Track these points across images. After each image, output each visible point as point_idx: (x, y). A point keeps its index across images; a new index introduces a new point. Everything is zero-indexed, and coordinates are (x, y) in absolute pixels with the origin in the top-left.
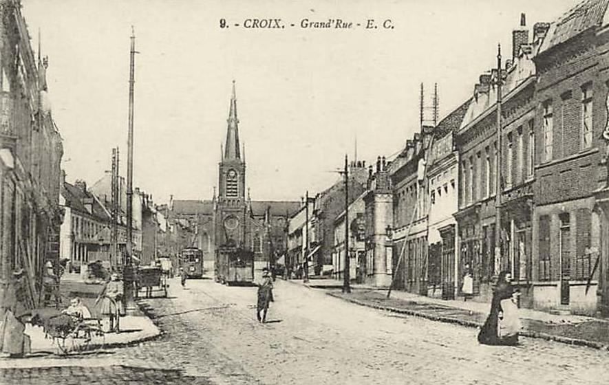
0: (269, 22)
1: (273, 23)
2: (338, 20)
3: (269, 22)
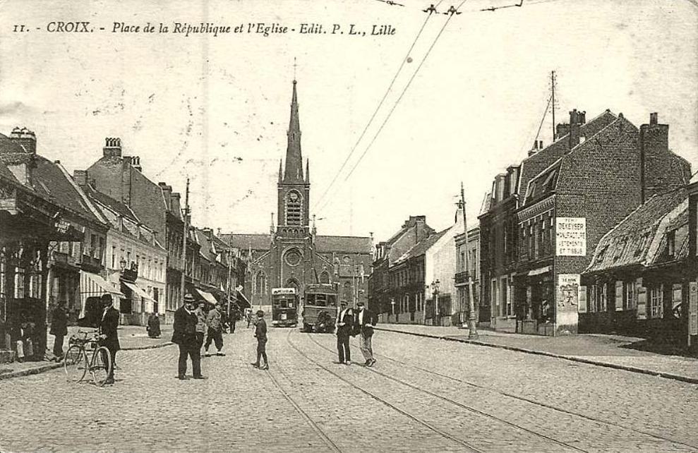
0: (75, 25)
1: (81, 26)
2: (59, 23)
3: (75, 25)
